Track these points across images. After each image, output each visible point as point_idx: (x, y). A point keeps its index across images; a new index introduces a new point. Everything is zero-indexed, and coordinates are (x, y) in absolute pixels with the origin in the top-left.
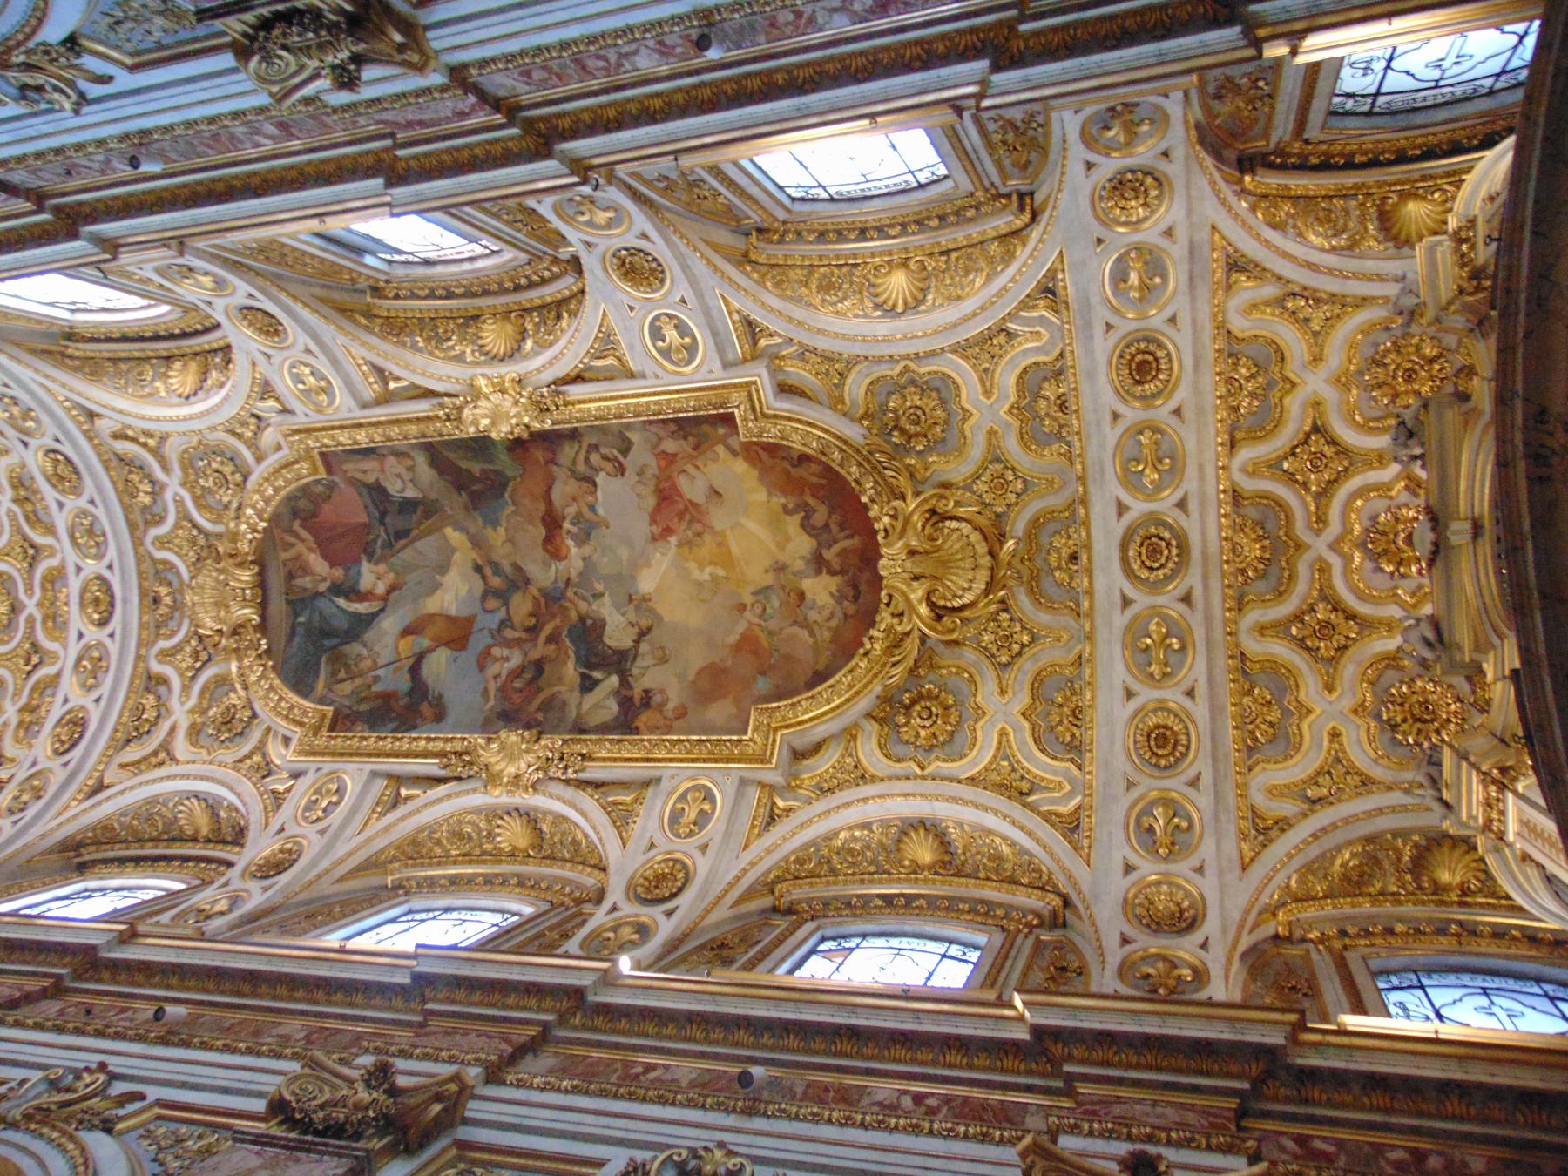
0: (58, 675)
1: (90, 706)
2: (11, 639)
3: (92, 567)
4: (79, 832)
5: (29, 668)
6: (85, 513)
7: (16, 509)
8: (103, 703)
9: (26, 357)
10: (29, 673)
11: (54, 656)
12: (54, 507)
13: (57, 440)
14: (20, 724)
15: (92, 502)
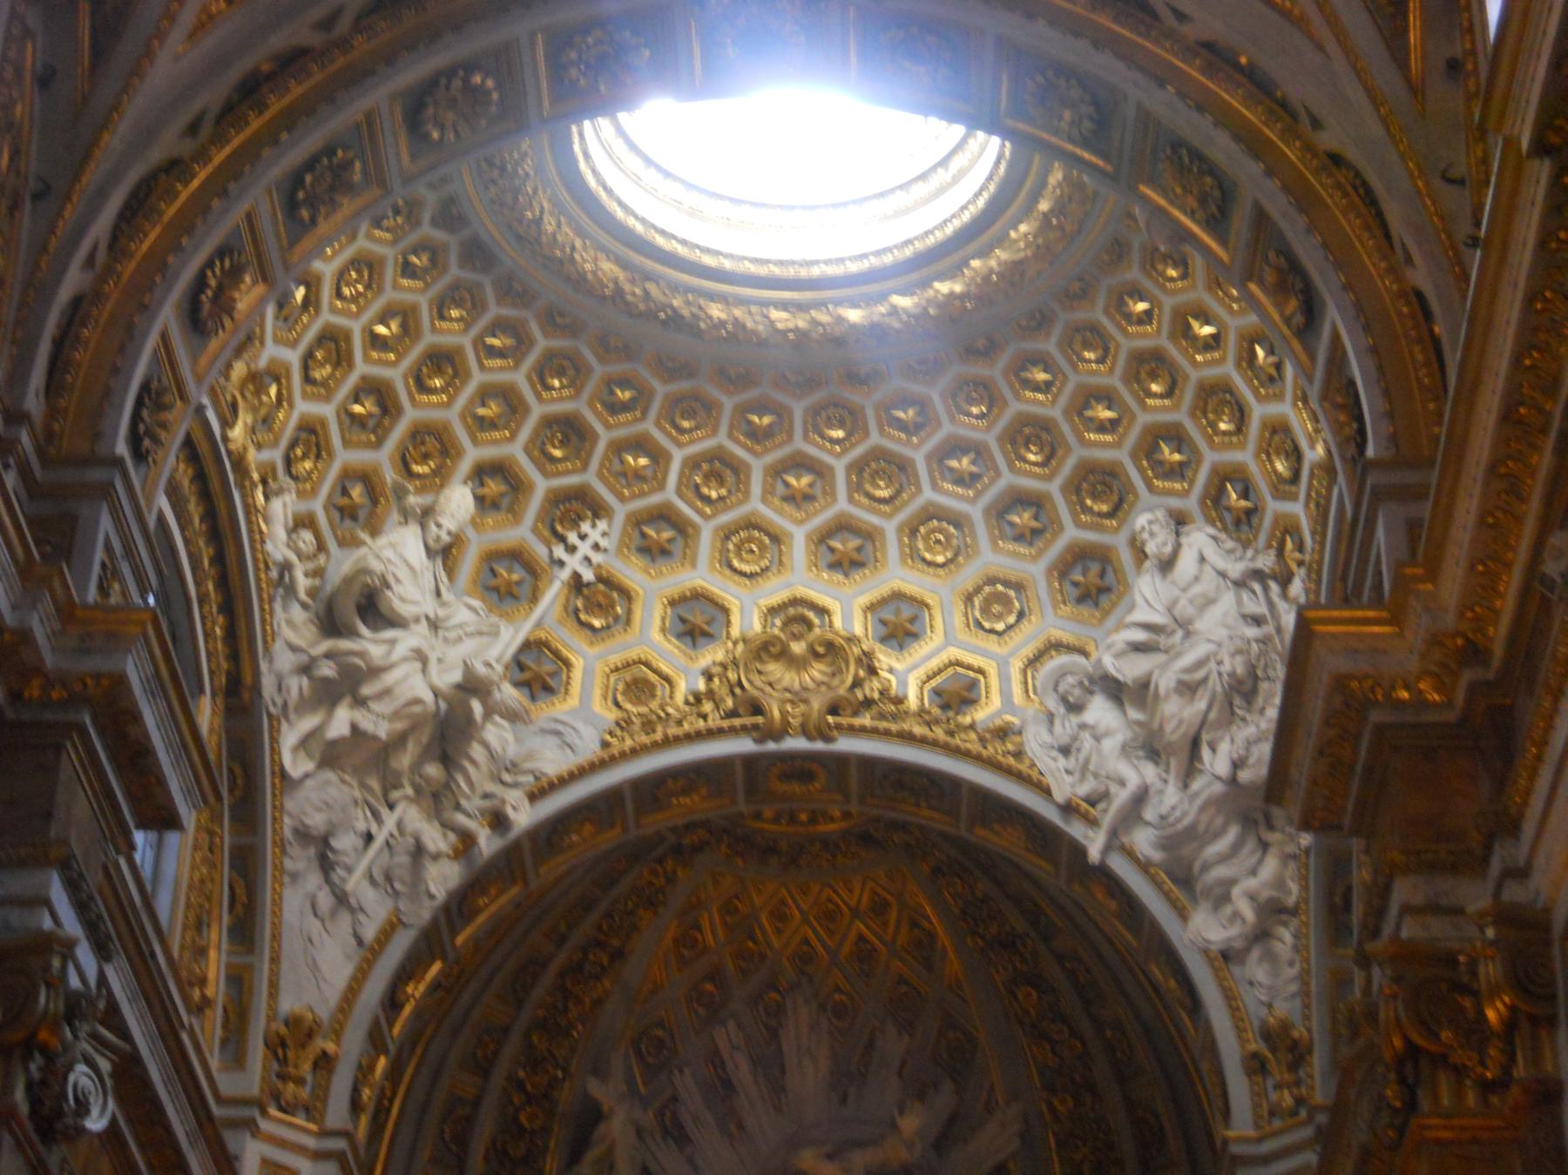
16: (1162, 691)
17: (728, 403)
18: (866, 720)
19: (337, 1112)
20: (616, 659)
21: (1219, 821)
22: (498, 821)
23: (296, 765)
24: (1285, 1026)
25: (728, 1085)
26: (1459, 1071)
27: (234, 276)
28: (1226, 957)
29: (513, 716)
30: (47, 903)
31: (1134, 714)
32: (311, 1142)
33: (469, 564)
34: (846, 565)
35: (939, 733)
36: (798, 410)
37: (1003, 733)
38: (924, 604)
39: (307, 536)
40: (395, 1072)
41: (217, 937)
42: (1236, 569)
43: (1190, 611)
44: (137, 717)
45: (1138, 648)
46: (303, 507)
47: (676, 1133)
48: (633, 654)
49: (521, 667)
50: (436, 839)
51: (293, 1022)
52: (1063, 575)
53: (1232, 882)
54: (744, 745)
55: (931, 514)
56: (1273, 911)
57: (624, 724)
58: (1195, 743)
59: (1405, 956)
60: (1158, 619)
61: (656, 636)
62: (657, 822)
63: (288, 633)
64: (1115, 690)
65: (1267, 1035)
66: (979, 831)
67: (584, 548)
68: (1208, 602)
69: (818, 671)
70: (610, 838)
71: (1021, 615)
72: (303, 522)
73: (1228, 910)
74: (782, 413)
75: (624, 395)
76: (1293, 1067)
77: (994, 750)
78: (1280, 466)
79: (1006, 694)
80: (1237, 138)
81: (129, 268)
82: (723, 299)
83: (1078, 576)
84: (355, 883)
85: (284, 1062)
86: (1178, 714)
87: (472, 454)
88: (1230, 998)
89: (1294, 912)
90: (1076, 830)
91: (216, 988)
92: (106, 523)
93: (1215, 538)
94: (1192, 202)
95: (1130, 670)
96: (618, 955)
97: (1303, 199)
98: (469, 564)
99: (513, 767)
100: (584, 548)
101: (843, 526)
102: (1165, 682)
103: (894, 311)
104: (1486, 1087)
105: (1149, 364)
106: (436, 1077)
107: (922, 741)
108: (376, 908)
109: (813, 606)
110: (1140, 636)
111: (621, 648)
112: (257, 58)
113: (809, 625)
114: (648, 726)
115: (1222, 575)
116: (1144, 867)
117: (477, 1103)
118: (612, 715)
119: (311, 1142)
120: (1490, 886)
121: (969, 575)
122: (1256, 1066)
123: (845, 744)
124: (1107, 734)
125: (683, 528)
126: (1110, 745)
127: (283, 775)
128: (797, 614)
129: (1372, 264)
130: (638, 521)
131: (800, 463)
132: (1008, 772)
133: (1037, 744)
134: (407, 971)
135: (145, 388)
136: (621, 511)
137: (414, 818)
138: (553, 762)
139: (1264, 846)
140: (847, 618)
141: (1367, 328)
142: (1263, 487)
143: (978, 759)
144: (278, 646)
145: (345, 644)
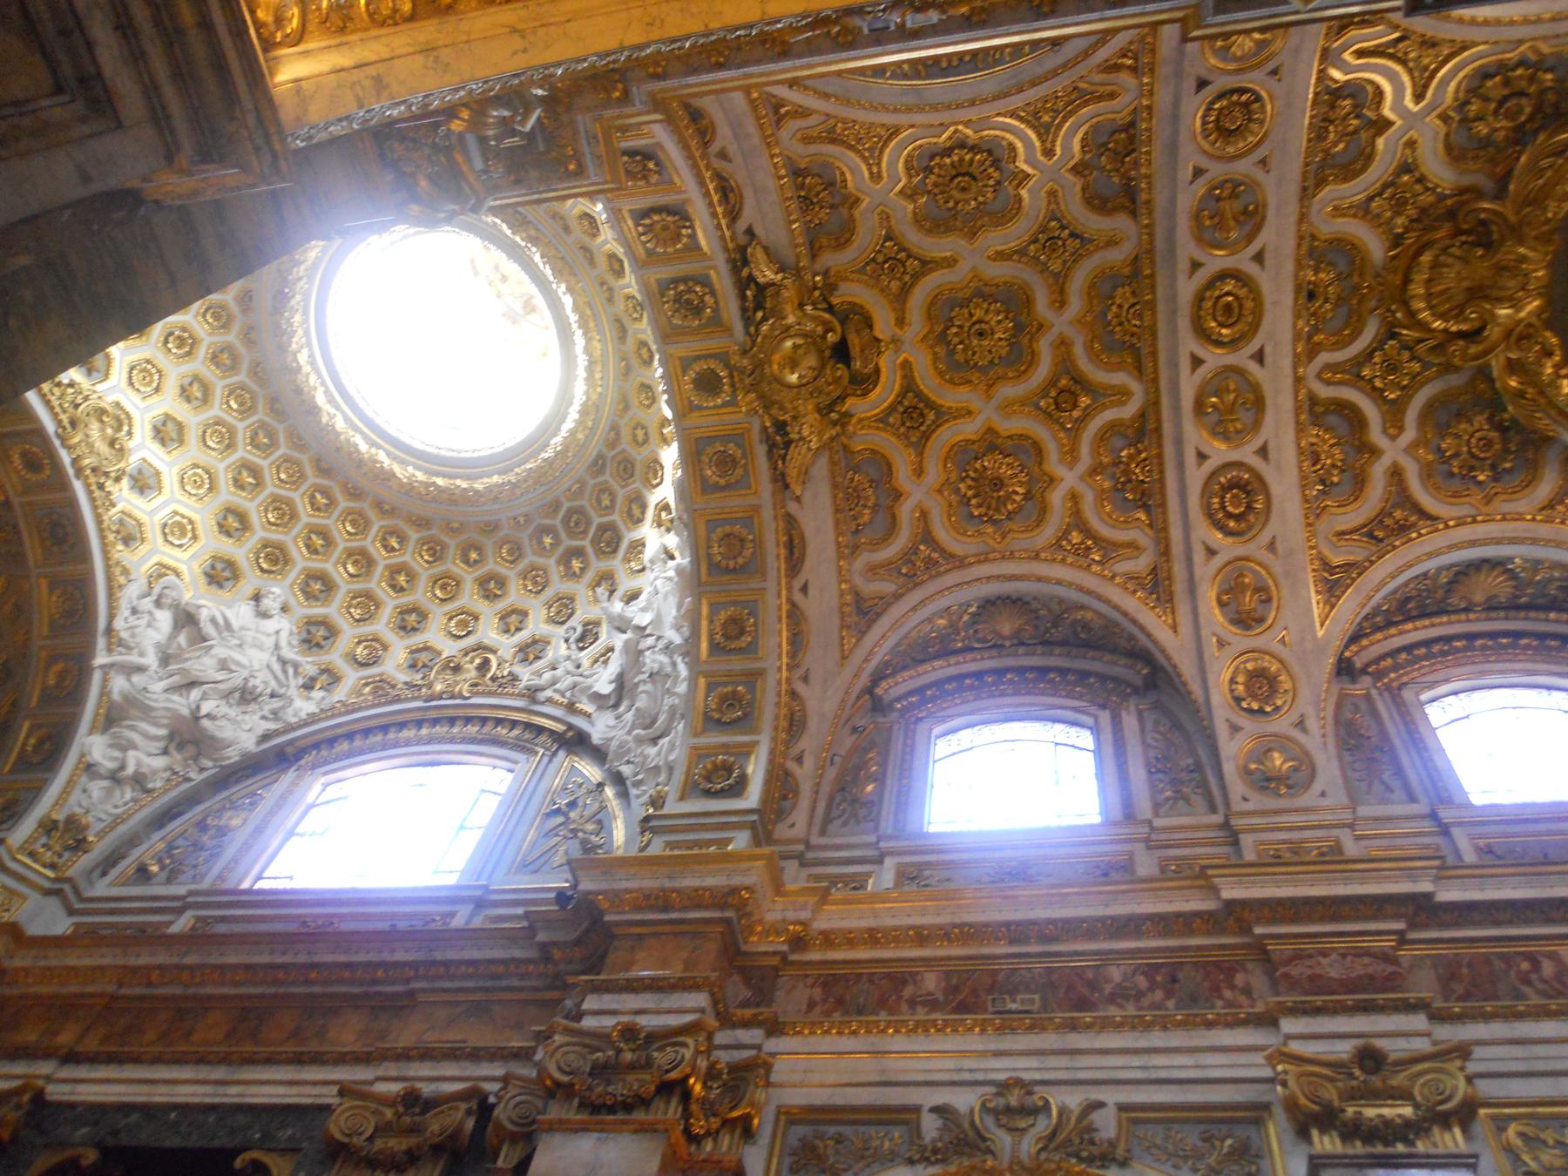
16: (213, 652)
21: (165, 721)
24: (87, 827)
28: (89, 769)
31: (182, 639)
37: (126, 572)
38: (160, 489)
43: (249, 640)
53: (135, 748)
56: (139, 780)
58: (193, 684)
60: (235, 624)
66: (44, 582)
68: (260, 648)
71: (180, 546)
73: (117, 754)
82: (306, 321)
83: (219, 566)
86: (204, 666)
88: (70, 783)
90: (101, 643)
93: (291, 633)
103: (331, 417)
109: (130, 426)
110: (220, 620)
113: (119, 429)
115: (277, 647)
116: (104, 692)
123: (78, 486)
124: (156, 629)
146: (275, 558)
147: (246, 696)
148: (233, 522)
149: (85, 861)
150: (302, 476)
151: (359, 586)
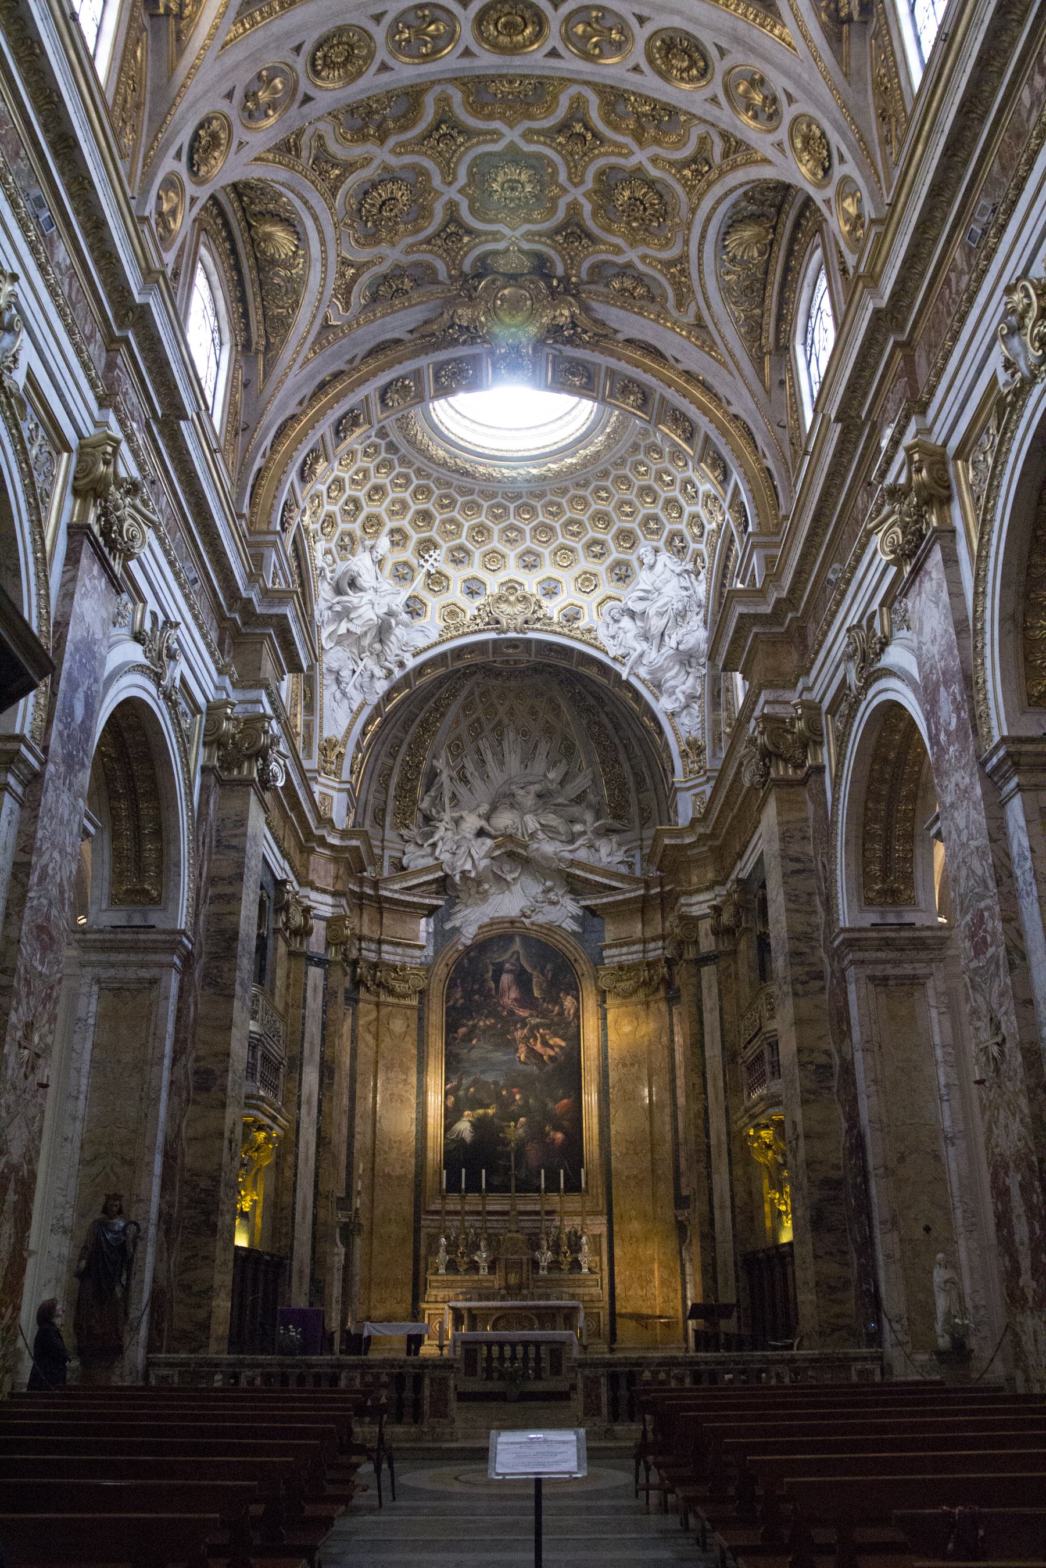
0: (601, 89)
1: (649, 28)
2: (551, 163)
3: (466, 34)
4: (818, 16)
5: (589, 136)
6: (394, 30)
7: (391, 142)
8: (645, 12)
9: (189, 58)
10: (596, 135)
11: (578, 101)
12: (385, 77)
13: (298, 49)
14: (657, 141)
15: (378, 18)
17: (486, 505)
18: (538, 626)
19: (345, 775)
20: (444, 603)
22: (401, 665)
23: (327, 645)
24: (696, 741)
25: (483, 761)
26: (786, 761)
27: (316, 460)
29: (406, 625)
30: (261, 702)
31: (639, 624)
32: (337, 785)
33: (388, 567)
34: (529, 567)
35: (566, 630)
36: (512, 507)
37: (589, 631)
39: (329, 557)
40: (363, 758)
41: (300, 709)
42: (678, 570)
44: (290, 631)
45: (641, 599)
46: (328, 546)
47: (464, 779)
48: (450, 601)
49: (408, 606)
50: (379, 673)
51: (328, 741)
52: (612, 571)
54: (493, 635)
55: (563, 547)
56: (692, 697)
57: (447, 628)
58: (662, 634)
59: (765, 718)
61: (459, 594)
62: (459, 664)
63: (322, 594)
64: (632, 614)
65: (688, 743)
67: (431, 560)
69: (520, 607)
70: (442, 671)
72: (328, 552)
74: (506, 509)
75: (446, 502)
76: (698, 755)
77: (586, 637)
78: (696, 530)
79: (591, 616)
80: (699, 408)
81: (278, 457)
82: (484, 465)
84: (350, 689)
85: (326, 756)
86: (656, 624)
87: (389, 525)
88: (674, 729)
89: (699, 698)
90: (617, 667)
91: (300, 729)
92: (274, 557)
94: (679, 432)
95: (637, 607)
96: (443, 715)
97: (724, 432)
98: (388, 567)
99: (406, 644)
100: (431, 560)
101: (529, 552)
102: (651, 612)
103: (549, 470)
104: (796, 767)
105: (646, 491)
106: (376, 760)
107: (560, 634)
108: (357, 698)
110: (642, 594)
111: (446, 598)
112: (325, 375)
114: (457, 629)
116: (643, 681)
117: (392, 768)
118: (444, 624)
119: (337, 785)
120: (797, 694)
121: (576, 570)
122: (684, 755)
123: (531, 635)
125: (468, 553)
126: (630, 635)
127: (323, 648)
128: (511, 586)
129: (751, 459)
130: (451, 550)
131: (512, 528)
132: (592, 645)
133: (603, 635)
134: (369, 721)
135: (286, 503)
136: (445, 546)
137: (369, 662)
138: (422, 643)
139: (688, 673)
140: (530, 586)
141: (749, 482)
142: (688, 537)
143: (580, 640)
144: (320, 600)
145: (345, 598)
146: (626, 537)
147: (681, 615)
148: (596, 548)
149: (708, 752)
150: (583, 498)
151: (661, 502)
